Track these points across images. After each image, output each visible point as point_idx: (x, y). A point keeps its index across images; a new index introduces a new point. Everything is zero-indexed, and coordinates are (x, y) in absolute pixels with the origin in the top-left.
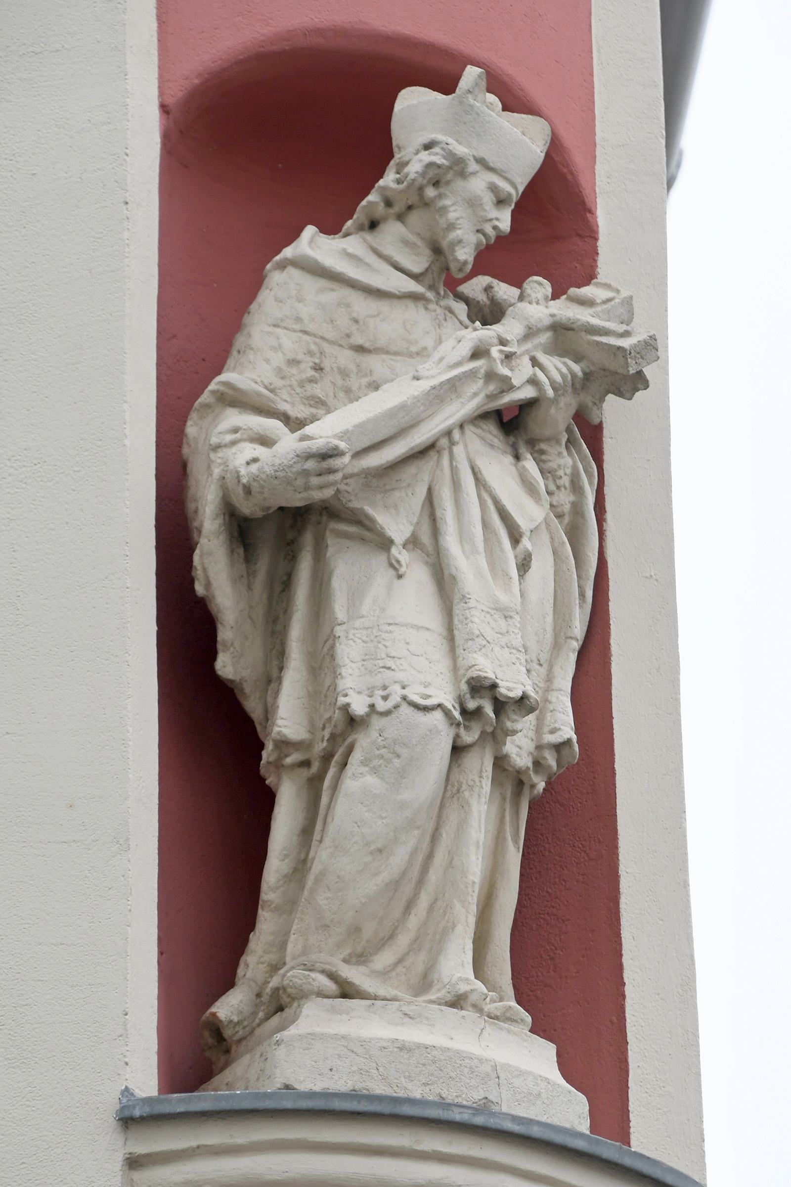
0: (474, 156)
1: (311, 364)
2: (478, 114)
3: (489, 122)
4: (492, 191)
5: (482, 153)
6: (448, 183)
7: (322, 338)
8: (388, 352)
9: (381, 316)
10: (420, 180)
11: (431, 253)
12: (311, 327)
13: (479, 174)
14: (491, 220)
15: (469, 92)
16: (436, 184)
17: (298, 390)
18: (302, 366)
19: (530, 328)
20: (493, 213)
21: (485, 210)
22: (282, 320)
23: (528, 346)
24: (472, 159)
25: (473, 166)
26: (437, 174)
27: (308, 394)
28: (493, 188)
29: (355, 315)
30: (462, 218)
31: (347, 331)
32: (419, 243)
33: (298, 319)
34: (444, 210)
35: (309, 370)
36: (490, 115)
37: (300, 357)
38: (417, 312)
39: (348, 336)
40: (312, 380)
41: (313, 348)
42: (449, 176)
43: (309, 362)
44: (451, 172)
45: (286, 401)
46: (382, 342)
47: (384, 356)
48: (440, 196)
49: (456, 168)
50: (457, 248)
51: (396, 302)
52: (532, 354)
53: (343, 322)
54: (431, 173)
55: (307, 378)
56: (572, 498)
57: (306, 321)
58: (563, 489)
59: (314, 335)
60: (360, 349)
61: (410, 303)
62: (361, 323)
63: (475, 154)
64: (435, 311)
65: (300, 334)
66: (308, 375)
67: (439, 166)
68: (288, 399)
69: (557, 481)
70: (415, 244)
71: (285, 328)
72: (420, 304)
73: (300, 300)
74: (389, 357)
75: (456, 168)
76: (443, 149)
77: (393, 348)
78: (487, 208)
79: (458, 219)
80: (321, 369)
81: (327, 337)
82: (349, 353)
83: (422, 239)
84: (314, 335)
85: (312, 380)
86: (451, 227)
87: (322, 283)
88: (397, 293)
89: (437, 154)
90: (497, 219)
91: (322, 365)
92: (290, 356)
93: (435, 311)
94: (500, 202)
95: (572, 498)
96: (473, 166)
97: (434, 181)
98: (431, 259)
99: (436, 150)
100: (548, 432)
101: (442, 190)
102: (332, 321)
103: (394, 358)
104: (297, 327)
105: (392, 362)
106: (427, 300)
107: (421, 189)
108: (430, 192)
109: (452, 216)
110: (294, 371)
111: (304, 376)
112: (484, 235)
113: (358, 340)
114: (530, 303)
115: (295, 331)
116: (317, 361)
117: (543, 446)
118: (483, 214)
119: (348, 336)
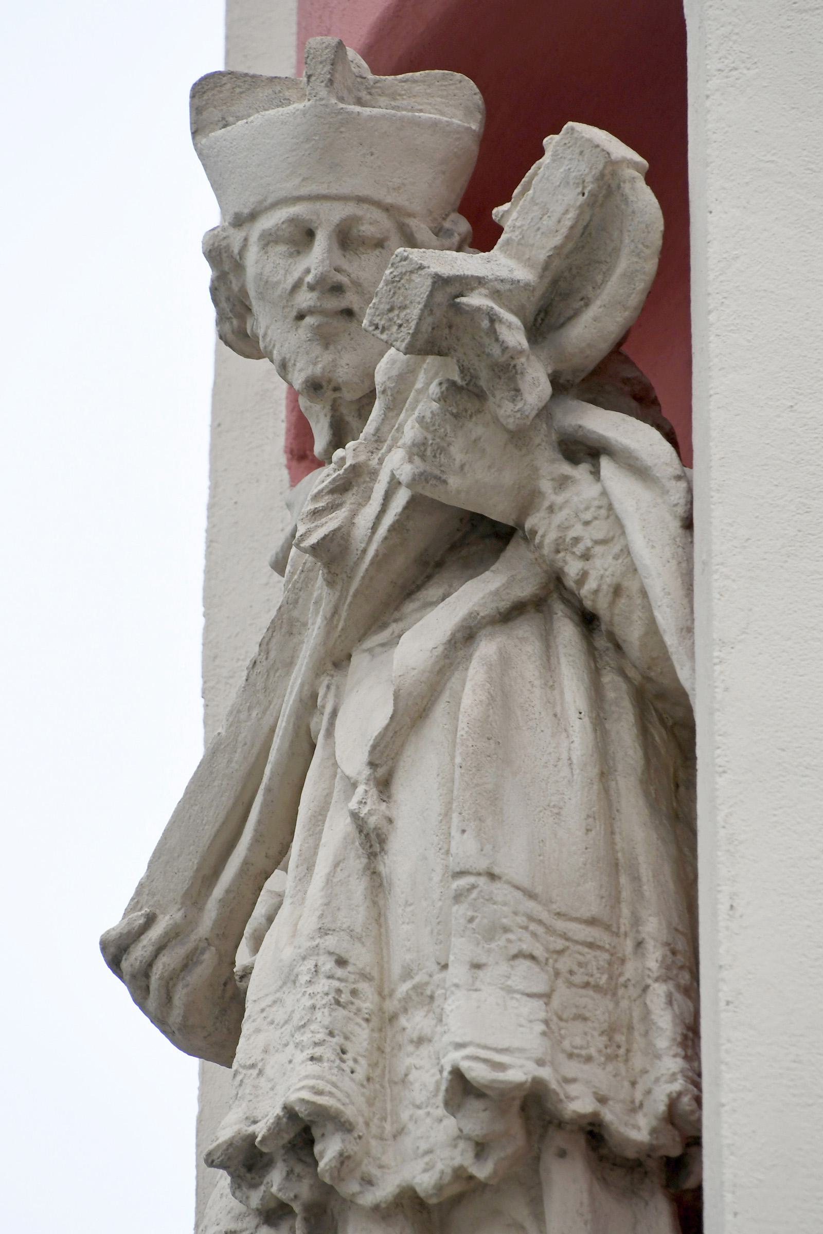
4: (276, 242)
6: (243, 292)
14: (297, 286)
21: (278, 283)
24: (232, 231)
28: (269, 239)
42: (235, 287)
44: (231, 277)
49: (226, 268)
58: (598, 549)
69: (575, 550)
90: (308, 271)
96: (236, 238)
112: (311, 311)
118: (279, 291)
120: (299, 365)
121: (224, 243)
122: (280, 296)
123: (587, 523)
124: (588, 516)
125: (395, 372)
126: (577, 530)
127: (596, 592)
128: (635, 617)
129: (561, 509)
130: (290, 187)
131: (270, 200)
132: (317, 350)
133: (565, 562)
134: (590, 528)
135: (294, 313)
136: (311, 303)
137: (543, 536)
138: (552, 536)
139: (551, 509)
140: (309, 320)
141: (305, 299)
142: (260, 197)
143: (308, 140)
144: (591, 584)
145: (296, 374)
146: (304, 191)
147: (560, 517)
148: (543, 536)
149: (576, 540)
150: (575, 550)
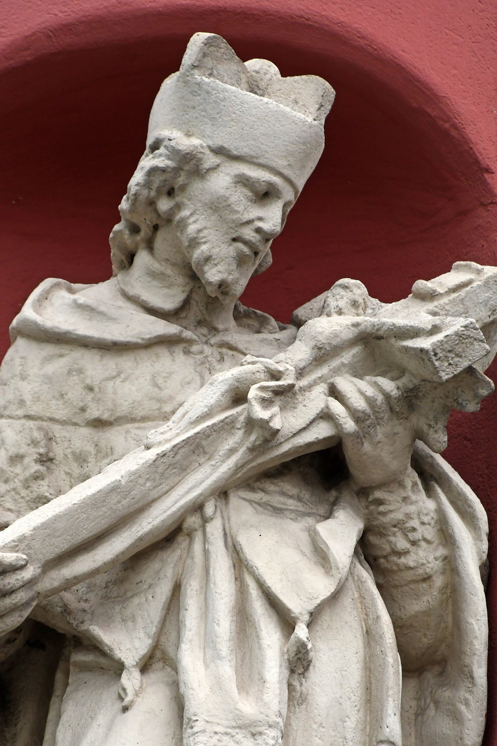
0: (209, 147)
1: (35, 456)
2: (208, 92)
3: (224, 99)
4: (245, 185)
5: (218, 142)
6: (183, 188)
7: (51, 419)
8: (133, 420)
9: (123, 376)
10: (145, 192)
11: (187, 280)
12: (34, 410)
13: (222, 168)
14: (249, 222)
15: (194, 67)
16: (171, 193)
17: (24, 493)
18: (26, 461)
19: (320, 349)
20: (254, 212)
21: (237, 212)
22: (5, 408)
23: (324, 370)
24: (208, 152)
25: (211, 160)
26: (165, 181)
27: (35, 495)
28: (243, 181)
29: (88, 381)
30: (205, 228)
31: (81, 404)
32: (169, 271)
33: (22, 403)
34: (183, 224)
35: (33, 464)
36: (224, 90)
37: (23, 450)
38: (173, 360)
39: (83, 410)
40: (37, 477)
41: (37, 435)
42: (181, 180)
43: (32, 453)
44: (182, 173)
45: (10, 510)
46: (124, 409)
47: (129, 426)
48: (178, 207)
50: (206, 268)
51: (143, 354)
52: (332, 380)
53: (75, 393)
54: (157, 181)
55: (31, 476)
56: (441, 552)
57: (28, 403)
58: (423, 544)
59: (41, 418)
60: (99, 424)
61: (163, 351)
62: (96, 390)
63: (210, 143)
64: (201, 352)
65: (23, 421)
66: (32, 471)
67: (164, 170)
68: (12, 507)
69: (409, 534)
70: (162, 274)
71: (10, 417)
72: (178, 350)
73: (23, 378)
74: (137, 425)
75: (186, 168)
76: (165, 146)
77: (140, 413)
78: (241, 208)
79: (199, 231)
80: (51, 460)
81: (57, 417)
82: (85, 431)
83: (174, 264)
84: (41, 418)
85: (37, 477)
86: (194, 243)
87: (50, 349)
88: (139, 341)
89: (160, 155)
90: (260, 219)
91: (51, 455)
92: (13, 451)
93: (201, 352)
94: (265, 195)
95: (441, 552)
96: (211, 160)
97: (165, 189)
98: (188, 288)
99: (162, 150)
100: (377, 475)
101: (178, 199)
102: (62, 395)
103: (142, 425)
104: (20, 412)
105: (137, 432)
106: (190, 342)
107: (152, 203)
108: (164, 205)
109: (192, 229)
110: (18, 469)
111: (27, 473)
112: (246, 243)
113: (94, 412)
114: (329, 315)
115: (19, 418)
116: (42, 450)
117: (378, 494)
118: (235, 217)
119: (83, 410)
120: (219, 267)
121: (200, 156)
122: (233, 221)
123: (423, 523)
124: (426, 519)
125: (334, 343)
126: (415, 523)
127: (409, 568)
128: (425, 599)
129: (412, 504)
130: (280, 164)
131: (261, 161)
132: (234, 267)
133: (394, 534)
134: (424, 528)
135: (234, 236)
136: (253, 240)
137: (391, 511)
138: (399, 516)
139: (405, 499)
140: (240, 245)
141: (249, 233)
142: (253, 153)
143: (304, 144)
144: (410, 560)
145: (214, 271)
146: (286, 172)
147: (412, 509)
148: (391, 511)
149: (414, 529)
150: (409, 534)
